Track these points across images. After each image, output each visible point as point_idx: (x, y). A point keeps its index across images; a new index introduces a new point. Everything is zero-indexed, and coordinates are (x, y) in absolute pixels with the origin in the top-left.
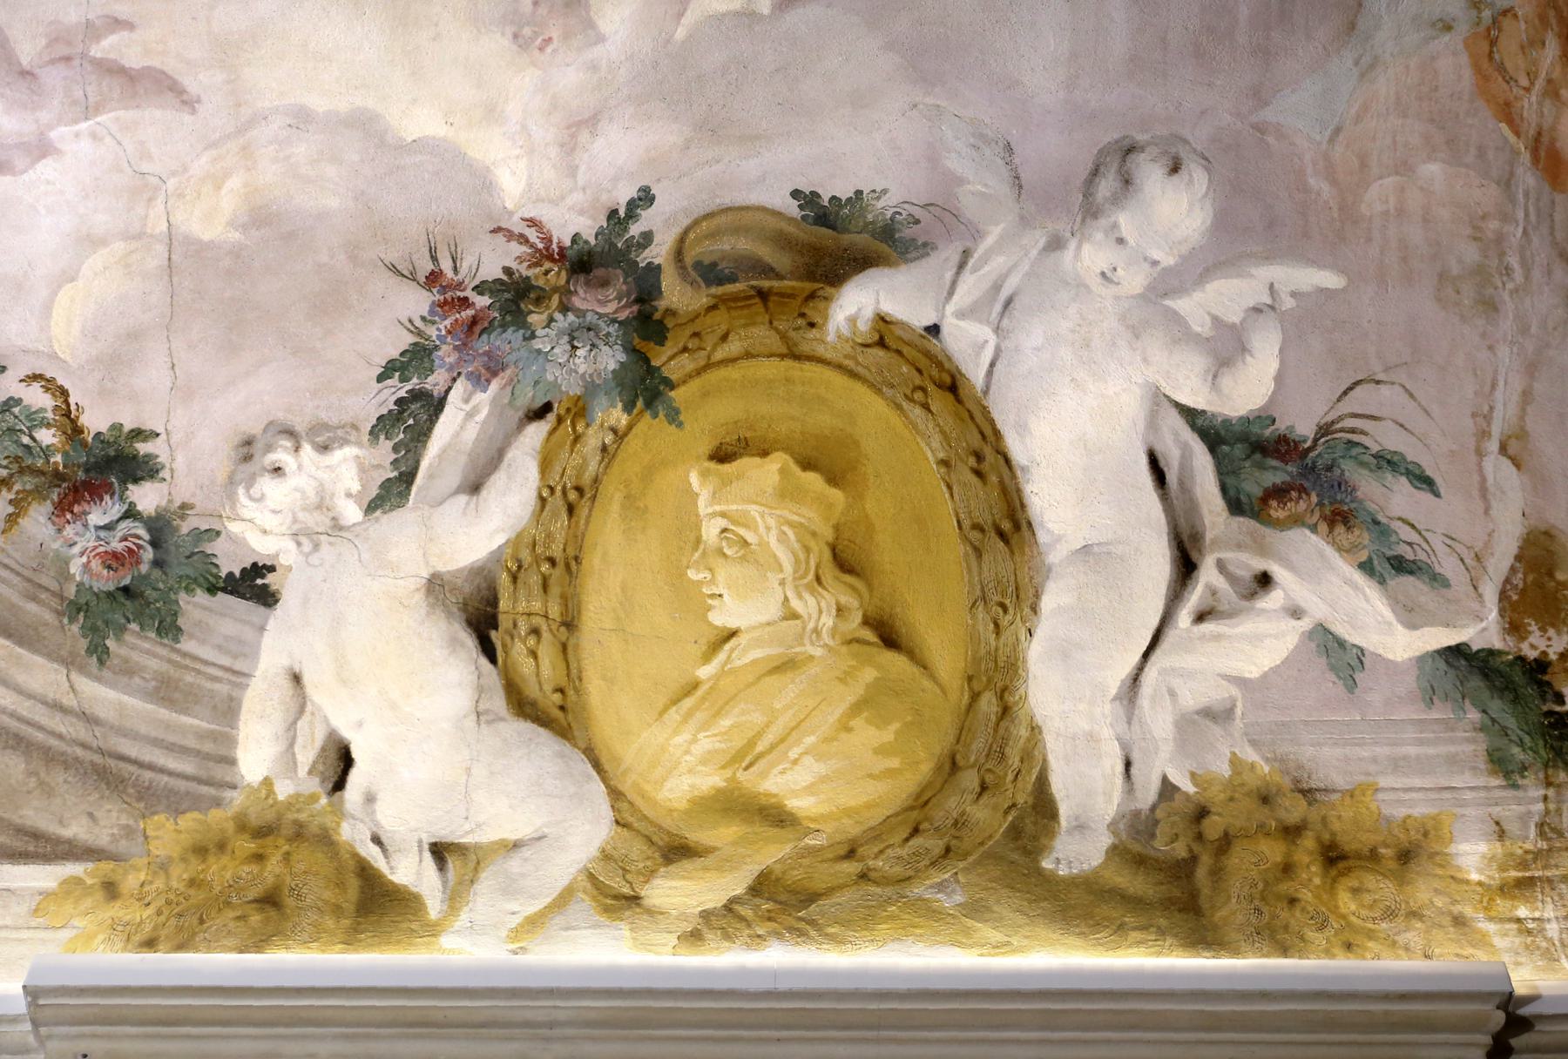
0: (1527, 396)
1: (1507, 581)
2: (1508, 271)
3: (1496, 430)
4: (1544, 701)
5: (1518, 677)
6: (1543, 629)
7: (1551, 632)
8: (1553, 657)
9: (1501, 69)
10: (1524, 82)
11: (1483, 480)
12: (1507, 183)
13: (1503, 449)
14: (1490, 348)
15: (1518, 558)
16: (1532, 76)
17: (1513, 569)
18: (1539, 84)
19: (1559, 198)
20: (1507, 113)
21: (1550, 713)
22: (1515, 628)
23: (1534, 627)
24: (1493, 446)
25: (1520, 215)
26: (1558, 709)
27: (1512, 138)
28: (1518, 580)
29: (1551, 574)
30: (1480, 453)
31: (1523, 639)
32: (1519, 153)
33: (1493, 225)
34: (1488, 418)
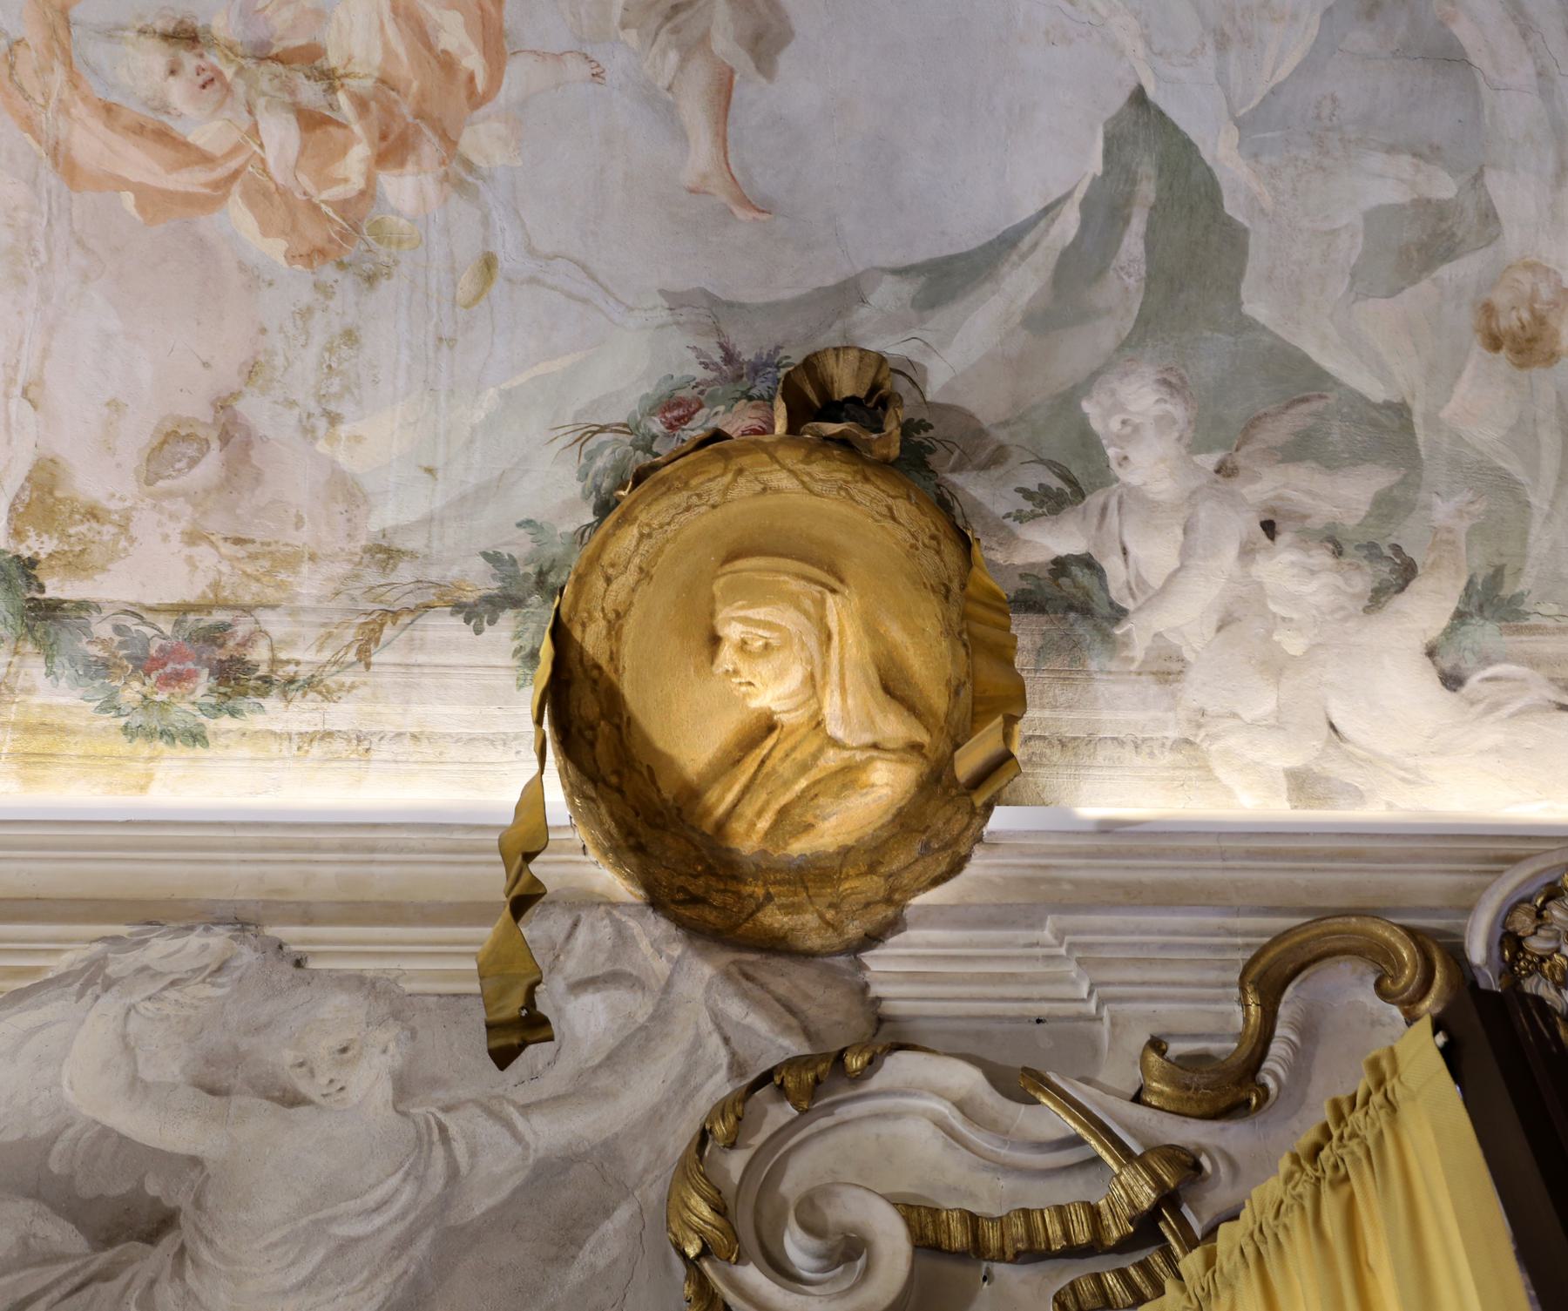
0: (46, 353)
1: (17, 496)
2: (35, 253)
3: (20, 380)
4: (29, 590)
5: (14, 572)
6: (39, 535)
7: (45, 537)
8: (43, 556)
9: (21, 89)
10: (40, 100)
11: (8, 418)
12: (33, 183)
13: (25, 393)
14: (20, 313)
15: (28, 479)
16: (47, 98)
17: (23, 488)
18: (53, 102)
19: (75, 196)
20: (28, 124)
21: (33, 599)
22: (17, 534)
23: (32, 533)
24: (17, 391)
25: (45, 208)
26: (38, 596)
27: (35, 146)
28: (25, 497)
29: (51, 493)
30: (7, 396)
31: (22, 541)
32: (41, 158)
33: (23, 215)
34: (16, 368)
